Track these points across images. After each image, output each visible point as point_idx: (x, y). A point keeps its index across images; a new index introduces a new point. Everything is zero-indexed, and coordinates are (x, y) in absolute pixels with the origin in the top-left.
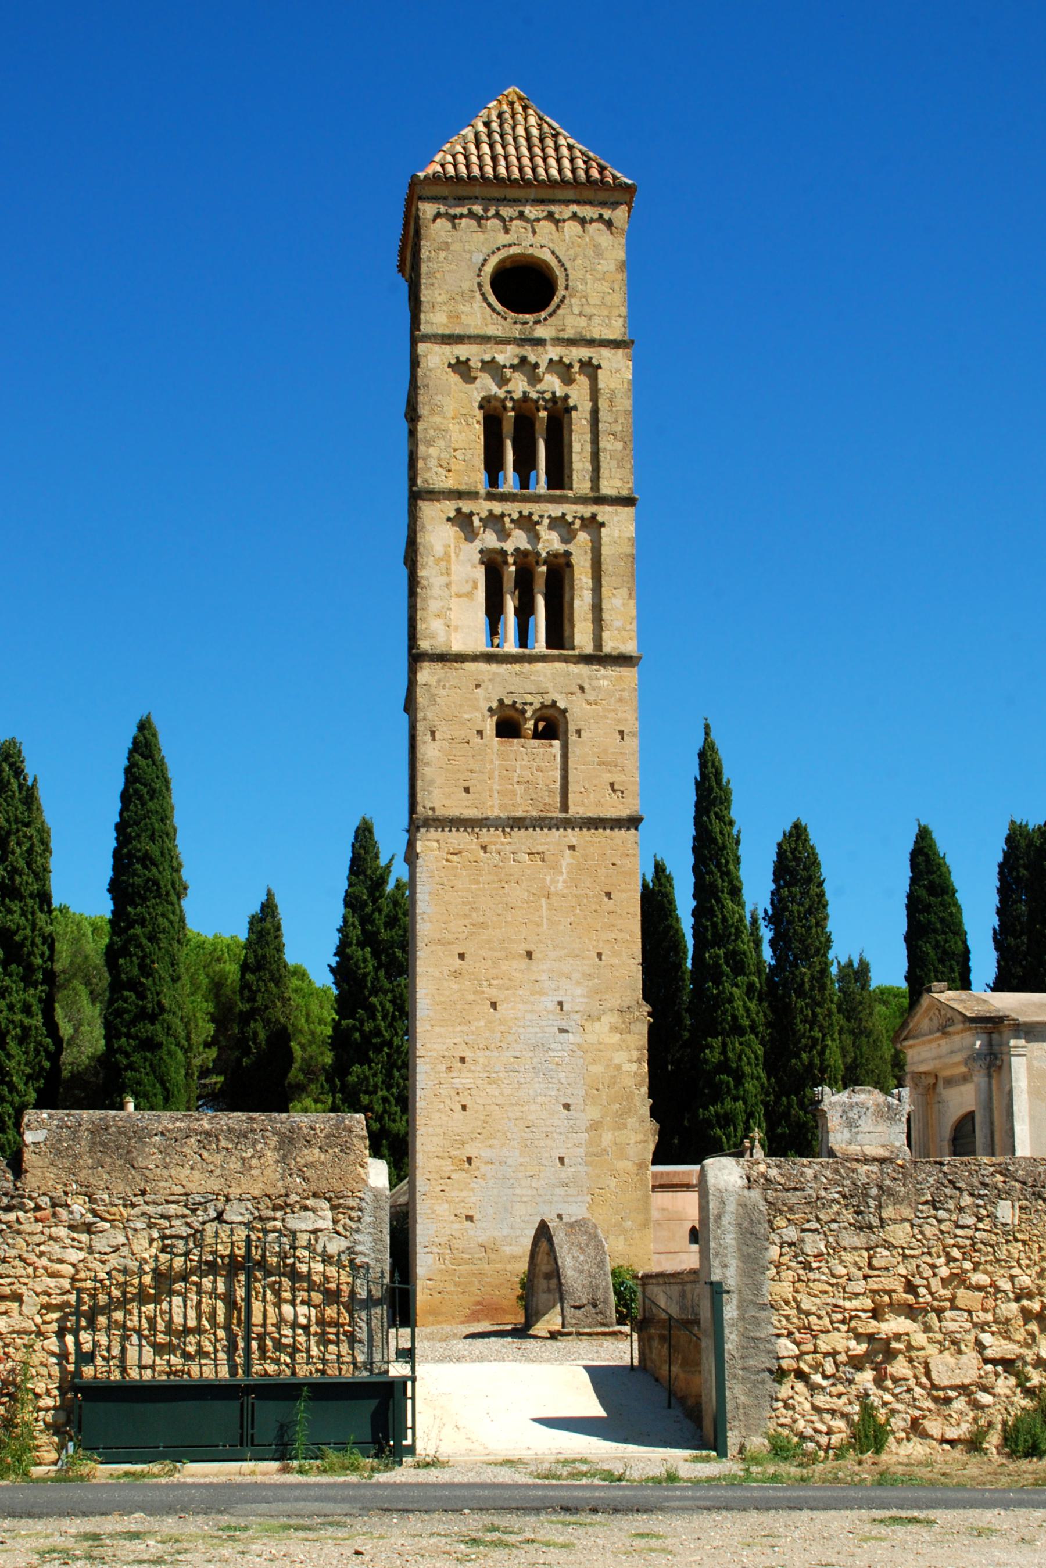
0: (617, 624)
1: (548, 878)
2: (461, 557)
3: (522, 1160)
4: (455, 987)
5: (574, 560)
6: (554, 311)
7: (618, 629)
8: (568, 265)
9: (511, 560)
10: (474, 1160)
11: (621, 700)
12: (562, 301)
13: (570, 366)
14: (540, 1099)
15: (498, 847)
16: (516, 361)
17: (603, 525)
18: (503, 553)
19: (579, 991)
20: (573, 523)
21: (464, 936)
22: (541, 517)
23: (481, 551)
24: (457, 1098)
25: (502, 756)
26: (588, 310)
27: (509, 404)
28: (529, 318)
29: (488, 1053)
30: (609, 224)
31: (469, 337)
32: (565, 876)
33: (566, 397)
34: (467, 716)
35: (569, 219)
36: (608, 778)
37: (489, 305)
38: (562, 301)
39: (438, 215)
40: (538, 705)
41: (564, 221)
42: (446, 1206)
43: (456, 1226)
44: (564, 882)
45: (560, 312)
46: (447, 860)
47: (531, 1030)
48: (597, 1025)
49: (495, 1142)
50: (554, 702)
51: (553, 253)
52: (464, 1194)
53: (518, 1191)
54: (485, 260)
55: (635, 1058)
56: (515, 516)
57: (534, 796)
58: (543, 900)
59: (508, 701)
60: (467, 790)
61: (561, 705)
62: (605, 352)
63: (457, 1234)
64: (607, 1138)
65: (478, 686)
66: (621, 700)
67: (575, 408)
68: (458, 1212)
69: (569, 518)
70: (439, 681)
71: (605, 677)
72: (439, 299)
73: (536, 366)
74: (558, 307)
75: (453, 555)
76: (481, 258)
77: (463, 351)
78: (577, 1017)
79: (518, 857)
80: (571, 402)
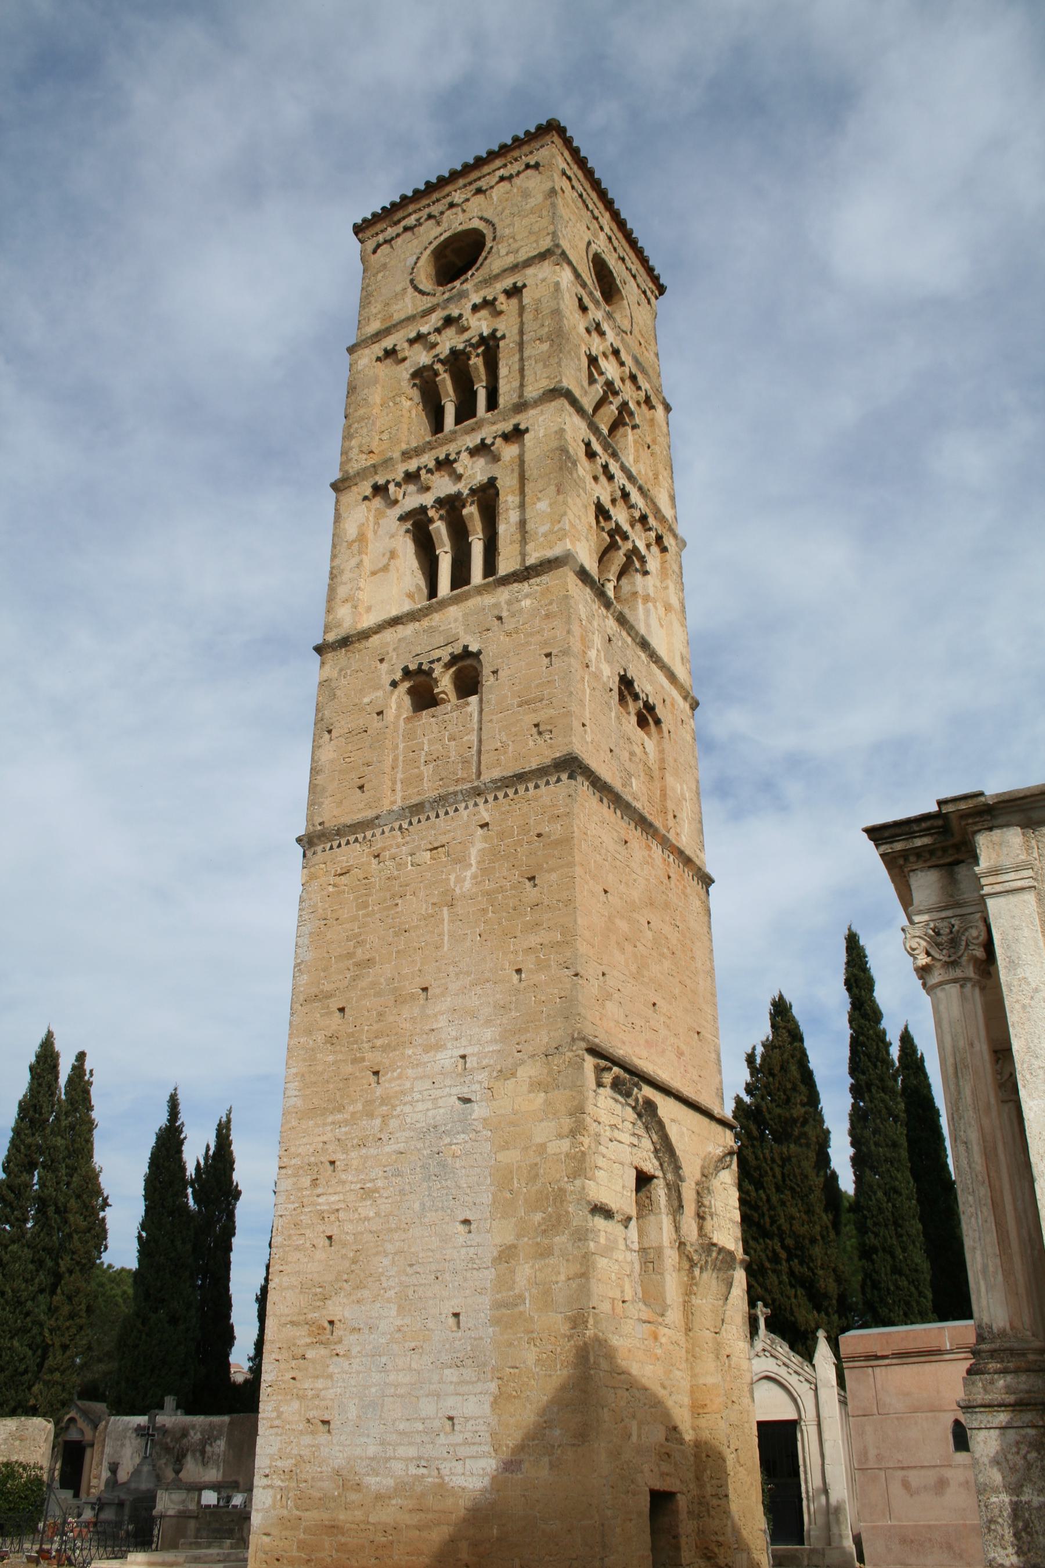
0: (543, 529)
1: (452, 877)
2: (380, 532)
3: (399, 1322)
4: (331, 1058)
5: (499, 484)
6: (481, 265)
7: (545, 535)
8: (495, 220)
9: (431, 513)
10: (337, 1325)
11: (547, 616)
12: (489, 253)
13: (495, 299)
14: (430, 1216)
15: (393, 851)
16: (440, 323)
17: (527, 430)
18: (423, 509)
19: (489, 1034)
20: (493, 444)
21: (346, 981)
22: (458, 453)
23: (402, 519)
24: (321, 1228)
25: (409, 736)
26: (515, 246)
27: (438, 366)
28: (457, 283)
29: (364, 1151)
30: (537, 166)
31: (395, 326)
32: (474, 869)
33: (495, 331)
34: (366, 700)
35: (498, 183)
36: (532, 718)
37: (422, 293)
38: (489, 253)
39: (379, 246)
40: (447, 658)
41: (492, 187)
42: (296, 1405)
43: (307, 1440)
44: (474, 877)
45: (488, 261)
46: (335, 886)
47: (420, 1106)
48: (510, 1083)
49: (366, 1293)
50: (466, 647)
51: (481, 218)
52: (320, 1384)
53: (392, 1377)
54: (418, 258)
55: (566, 1130)
56: (432, 465)
57: (444, 774)
58: (445, 909)
59: (413, 667)
60: (361, 787)
61: (474, 648)
62: (530, 271)
63: (306, 1453)
64: (524, 1271)
65: (382, 661)
66: (547, 616)
67: (503, 337)
68: (310, 1414)
69: (488, 441)
70: (341, 670)
71: (527, 596)
72: (374, 311)
73: (461, 316)
74: (486, 258)
75: (370, 535)
76: (415, 258)
77: (388, 343)
78: (482, 1076)
79: (417, 859)
80: (499, 334)
